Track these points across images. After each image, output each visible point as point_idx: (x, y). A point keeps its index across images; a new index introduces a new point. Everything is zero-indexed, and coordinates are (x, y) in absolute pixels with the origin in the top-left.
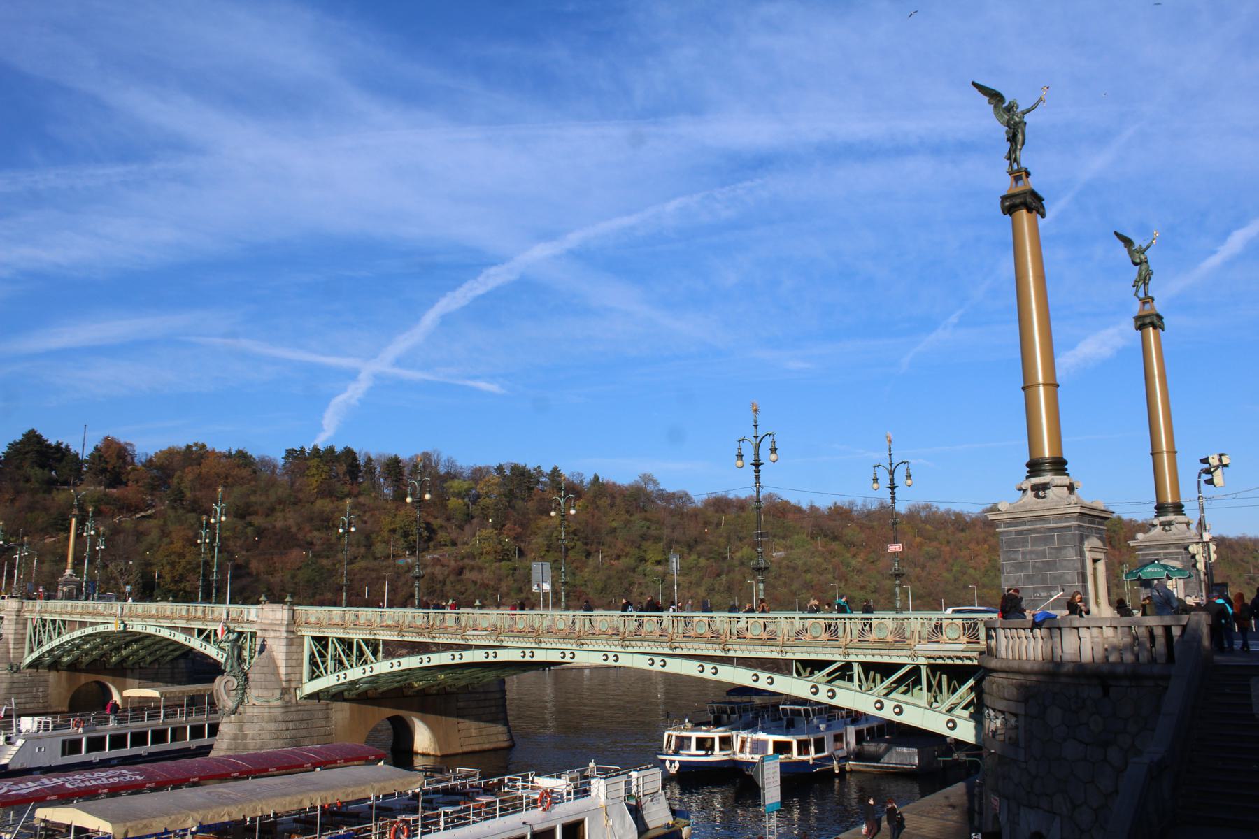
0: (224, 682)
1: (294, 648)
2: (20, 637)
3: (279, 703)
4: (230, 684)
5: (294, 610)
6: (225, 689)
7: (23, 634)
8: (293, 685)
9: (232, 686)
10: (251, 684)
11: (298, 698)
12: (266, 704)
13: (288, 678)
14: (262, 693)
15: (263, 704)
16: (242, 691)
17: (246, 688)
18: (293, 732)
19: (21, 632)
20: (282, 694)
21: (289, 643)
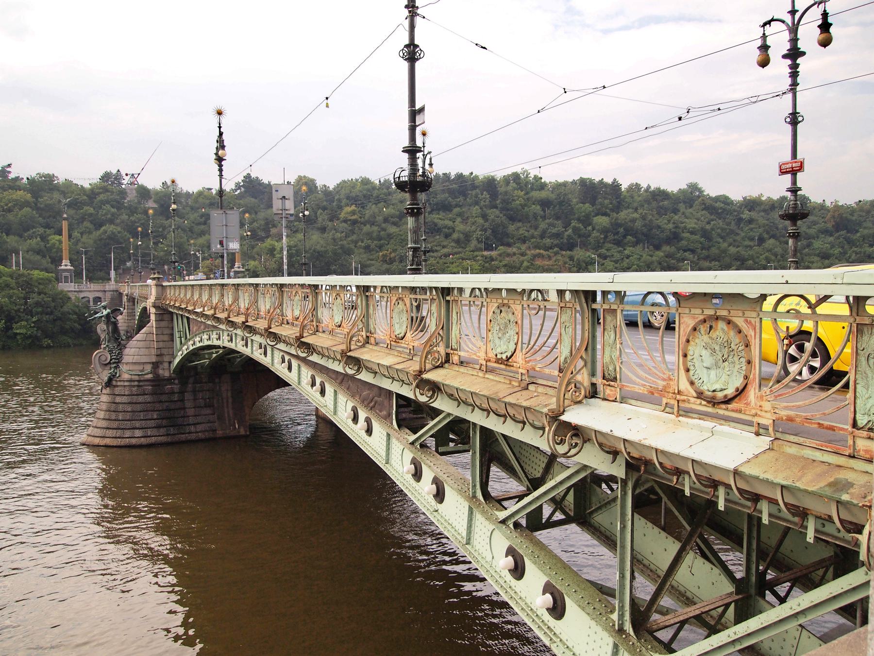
0: (99, 355)
1: (163, 324)
2: (130, 311)
3: (150, 376)
4: (103, 358)
5: (162, 286)
6: (99, 360)
7: (132, 309)
8: (166, 359)
9: (106, 360)
10: (126, 359)
11: (172, 372)
12: (137, 377)
13: (159, 353)
14: (131, 367)
15: (133, 377)
16: (114, 365)
17: (118, 362)
18: (167, 404)
19: (131, 307)
20: (152, 368)
21: (158, 319)
